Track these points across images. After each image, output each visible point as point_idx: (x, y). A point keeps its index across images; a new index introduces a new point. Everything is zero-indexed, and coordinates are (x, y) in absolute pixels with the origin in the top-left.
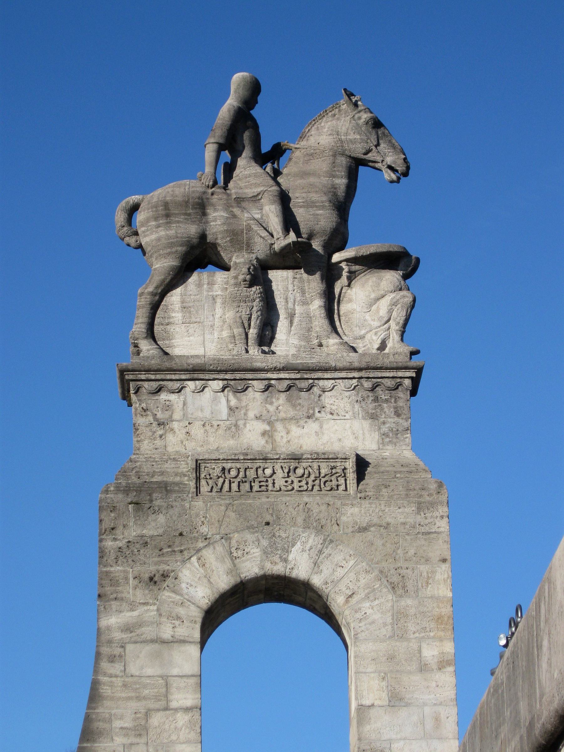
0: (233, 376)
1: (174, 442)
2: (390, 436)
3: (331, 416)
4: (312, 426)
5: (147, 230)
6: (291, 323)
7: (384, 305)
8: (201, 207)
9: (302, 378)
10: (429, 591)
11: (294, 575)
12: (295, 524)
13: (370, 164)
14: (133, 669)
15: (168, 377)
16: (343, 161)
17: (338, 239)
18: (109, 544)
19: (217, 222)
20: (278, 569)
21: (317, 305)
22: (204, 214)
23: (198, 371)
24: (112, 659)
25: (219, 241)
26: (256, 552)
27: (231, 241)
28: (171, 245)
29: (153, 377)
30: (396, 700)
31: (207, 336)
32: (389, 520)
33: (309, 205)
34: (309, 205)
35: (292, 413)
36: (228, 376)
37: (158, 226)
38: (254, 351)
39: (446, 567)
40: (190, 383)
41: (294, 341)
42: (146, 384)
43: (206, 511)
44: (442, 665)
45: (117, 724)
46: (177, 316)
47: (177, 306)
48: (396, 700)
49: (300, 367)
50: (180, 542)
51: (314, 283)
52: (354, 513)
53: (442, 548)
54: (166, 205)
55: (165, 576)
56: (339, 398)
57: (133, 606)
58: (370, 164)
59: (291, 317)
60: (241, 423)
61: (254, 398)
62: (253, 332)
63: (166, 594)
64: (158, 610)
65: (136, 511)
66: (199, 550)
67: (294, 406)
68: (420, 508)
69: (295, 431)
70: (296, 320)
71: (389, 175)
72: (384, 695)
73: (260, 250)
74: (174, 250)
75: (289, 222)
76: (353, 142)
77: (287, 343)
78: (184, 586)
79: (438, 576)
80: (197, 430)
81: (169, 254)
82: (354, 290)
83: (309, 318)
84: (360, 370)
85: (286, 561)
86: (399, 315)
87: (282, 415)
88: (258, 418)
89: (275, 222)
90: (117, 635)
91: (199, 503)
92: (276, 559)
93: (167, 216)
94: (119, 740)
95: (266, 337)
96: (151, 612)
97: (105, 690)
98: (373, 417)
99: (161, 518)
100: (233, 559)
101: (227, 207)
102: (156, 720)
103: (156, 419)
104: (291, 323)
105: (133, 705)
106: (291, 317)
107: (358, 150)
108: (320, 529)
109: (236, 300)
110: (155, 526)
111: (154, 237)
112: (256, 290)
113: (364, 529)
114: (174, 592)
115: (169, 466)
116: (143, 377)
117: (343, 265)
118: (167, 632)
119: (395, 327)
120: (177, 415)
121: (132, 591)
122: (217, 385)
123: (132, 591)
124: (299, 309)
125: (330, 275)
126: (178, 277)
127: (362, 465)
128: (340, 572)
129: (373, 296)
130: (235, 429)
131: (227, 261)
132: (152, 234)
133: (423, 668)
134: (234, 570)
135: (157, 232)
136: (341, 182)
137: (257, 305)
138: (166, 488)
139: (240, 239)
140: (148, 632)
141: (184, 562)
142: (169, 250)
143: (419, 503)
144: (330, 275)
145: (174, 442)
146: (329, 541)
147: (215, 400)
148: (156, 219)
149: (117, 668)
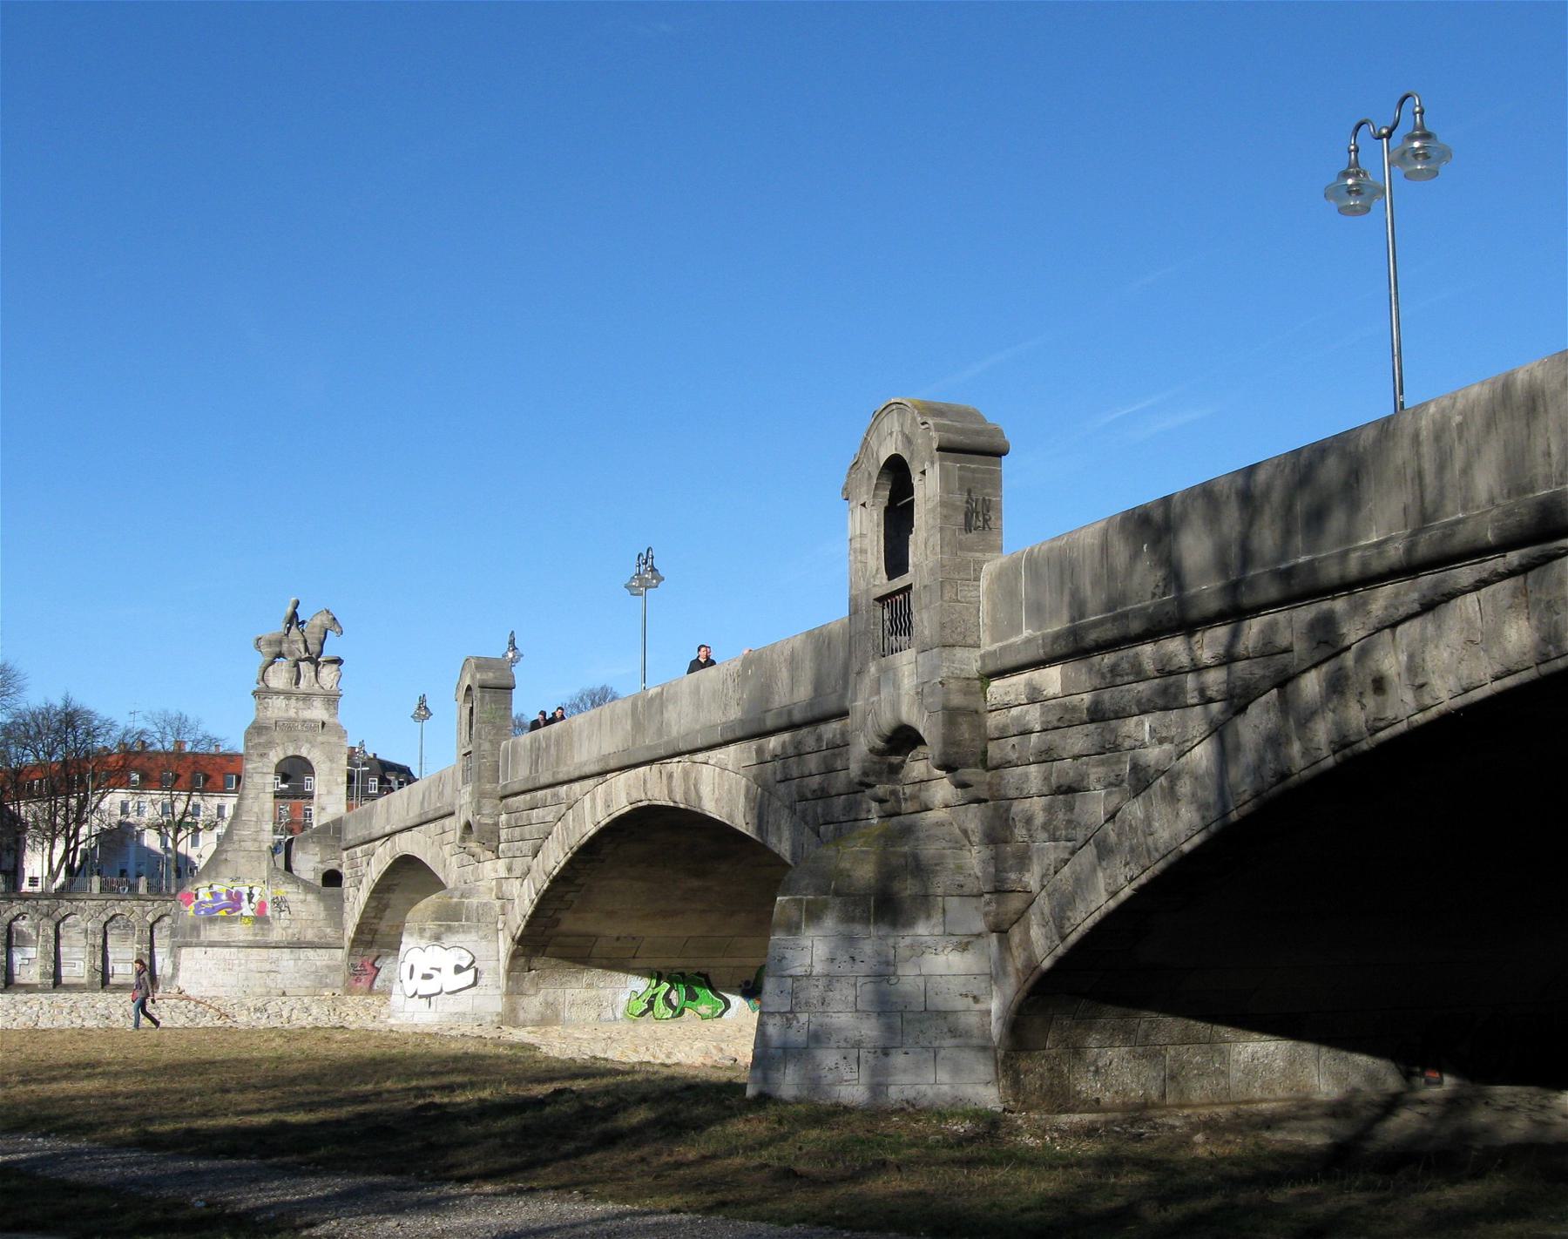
0: (287, 695)
8: (280, 642)
9: (307, 697)
19: (285, 647)
23: (278, 693)
30: (329, 793)
43: (277, 736)
48: (329, 793)
50: (270, 744)
51: (312, 667)
52: (320, 739)
56: (318, 703)
61: (293, 701)
73: (297, 655)
75: (307, 649)
77: (303, 684)
95: (297, 683)
121: (255, 758)
125: (317, 665)
126: (272, 663)
138: (267, 728)
139: (291, 653)
144: (317, 665)
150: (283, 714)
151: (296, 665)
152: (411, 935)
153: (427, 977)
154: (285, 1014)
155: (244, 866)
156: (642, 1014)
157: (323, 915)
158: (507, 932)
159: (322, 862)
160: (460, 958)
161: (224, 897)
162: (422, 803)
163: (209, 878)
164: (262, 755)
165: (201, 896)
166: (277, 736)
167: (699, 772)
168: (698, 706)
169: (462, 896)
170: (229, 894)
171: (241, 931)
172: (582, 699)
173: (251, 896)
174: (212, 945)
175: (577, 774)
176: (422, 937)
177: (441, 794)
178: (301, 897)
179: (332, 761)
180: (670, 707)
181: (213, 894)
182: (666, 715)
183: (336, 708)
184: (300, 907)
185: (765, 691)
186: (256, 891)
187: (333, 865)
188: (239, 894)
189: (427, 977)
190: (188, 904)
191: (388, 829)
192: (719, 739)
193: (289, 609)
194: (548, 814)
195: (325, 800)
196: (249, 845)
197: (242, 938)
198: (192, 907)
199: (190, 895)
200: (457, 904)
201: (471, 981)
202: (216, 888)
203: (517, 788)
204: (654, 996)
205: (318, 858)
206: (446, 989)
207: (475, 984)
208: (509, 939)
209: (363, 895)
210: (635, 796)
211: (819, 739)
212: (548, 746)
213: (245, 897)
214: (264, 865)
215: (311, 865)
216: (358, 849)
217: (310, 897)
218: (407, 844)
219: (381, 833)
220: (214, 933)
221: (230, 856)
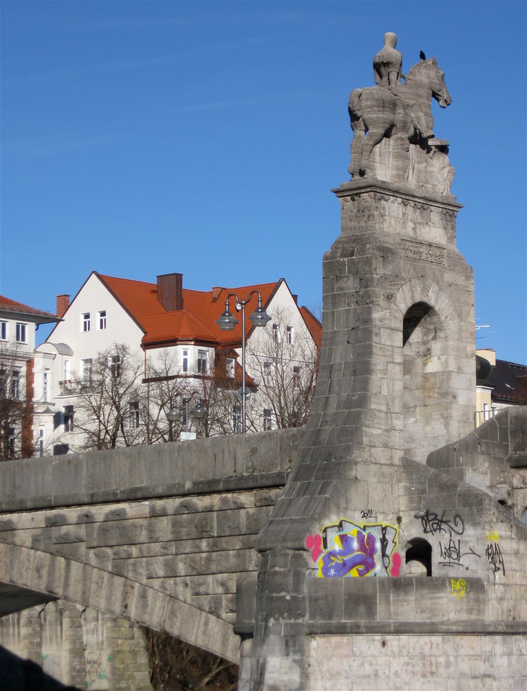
2: (451, 239)
3: (432, 225)
5: (372, 111)
6: (413, 172)
11: (429, 304)
12: (430, 279)
13: (437, 96)
15: (386, 193)
22: (395, 110)
25: (397, 125)
27: (402, 126)
28: (384, 123)
29: (381, 191)
31: (387, 172)
32: (457, 282)
35: (421, 221)
36: (404, 197)
37: (379, 111)
39: (473, 309)
40: (391, 197)
41: (414, 182)
42: (378, 194)
45: (379, 367)
46: (377, 158)
47: (378, 154)
49: (428, 198)
53: (472, 300)
58: (437, 96)
60: (406, 221)
64: (390, 312)
65: (384, 260)
66: (402, 285)
67: (422, 217)
70: (415, 171)
71: (442, 103)
72: (456, 367)
74: (385, 125)
76: (436, 84)
78: (398, 302)
79: (471, 313)
81: (383, 127)
82: (434, 161)
84: (444, 204)
85: (428, 296)
87: (419, 221)
88: (412, 220)
90: (378, 323)
92: (425, 294)
93: (383, 107)
94: (379, 375)
96: (387, 313)
98: (445, 228)
100: (413, 291)
103: (380, 214)
104: (413, 172)
105: (383, 358)
111: (375, 116)
113: (450, 285)
114: (395, 304)
116: (378, 191)
117: (433, 148)
122: (400, 200)
128: (444, 305)
129: (442, 166)
131: (392, 133)
132: (374, 114)
134: (413, 298)
135: (377, 114)
142: (383, 125)
143: (466, 276)
147: (398, 208)
148: (378, 107)
171: (450, 605)
174: (403, 629)
197: (453, 616)
198: (319, 563)
220: (408, 608)
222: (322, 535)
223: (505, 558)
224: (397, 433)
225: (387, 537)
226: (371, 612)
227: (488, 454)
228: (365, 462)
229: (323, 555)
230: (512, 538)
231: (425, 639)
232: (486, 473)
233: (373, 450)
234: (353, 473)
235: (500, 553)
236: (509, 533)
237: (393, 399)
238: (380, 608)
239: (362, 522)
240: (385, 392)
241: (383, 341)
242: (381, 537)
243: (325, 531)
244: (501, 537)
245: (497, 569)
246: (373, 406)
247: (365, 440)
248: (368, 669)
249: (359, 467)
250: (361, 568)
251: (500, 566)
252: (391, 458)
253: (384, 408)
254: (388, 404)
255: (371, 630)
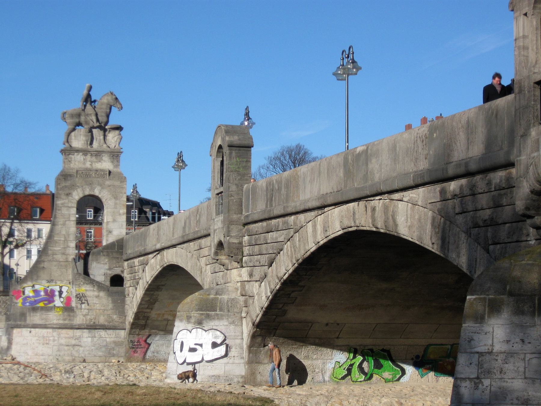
0: (85, 152)
1: (72, 165)
4: (100, 163)
7: (116, 138)
8: (79, 115)
9: (98, 154)
10: (122, 199)
14: (63, 212)
16: (109, 106)
17: (107, 123)
18: (59, 187)
19: (82, 119)
20: (92, 193)
21: (102, 137)
23: (78, 151)
24: (59, 210)
26: (88, 190)
30: (114, 221)
33: (102, 116)
34: (102, 116)
38: (89, 147)
44: (124, 214)
45: (60, 223)
46: (73, 138)
48: (114, 221)
50: (73, 187)
51: (102, 133)
52: (108, 183)
54: (72, 115)
55: (70, 194)
56: (106, 158)
57: (63, 199)
59: (97, 139)
62: (89, 143)
63: (70, 198)
68: (121, 182)
69: (97, 164)
73: (91, 124)
75: (98, 120)
77: (95, 144)
80: (77, 163)
83: (100, 140)
86: (118, 140)
89: (95, 120)
91: (77, 179)
94: (60, 226)
95: (91, 143)
96: (66, 201)
97: (57, 216)
98: (112, 162)
99: (69, 182)
101: (85, 116)
102: (67, 222)
106: (97, 139)
107: (112, 104)
108: (101, 185)
109: (85, 136)
110: (68, 183)
112: (90, 134)
113: (109, 186)
115: (71, 171)
118: (70, 205)
119: (118, 143)
120: (73, 160)
122: (81, 154)
123: (63, 197)
124: (98, 138)
125: (105, 130)
126: (74, 130)
127: (110, 172)
130: (84, 163)
133: (120, 214)
134: (84, 193)
136: (108, 111)
137: (90, 137)
138: (70, 176)
139: (87, 123)
140: (66, 205)
141: (74, 191)
145: (72, 165)
146: (102, 188)
149: (59, 212)
150: (81, 166)
151: (91, 131)
152: (181, 320)
153: (192, 350)
154: (86, 375)
155: (56, 272)
156: (343, 378)
157: (111, 306)
158: (249, 319)
159: (110, 269)
160: (216, 337)
161: (42, 293)
162: (184, 228)
163: (32, 280)
164: (68, 195)
165: (27, 293)
166: (78, 181)
167: (396, 206)
168: (395, 160)
169: (217, 294)
170: (46, 291)
171: (54, 317)
172: (282, 154)
173: (61, 292)
174: (35, 326)
175: (302, 208)
176: (189, 322)
177: (198, 221)
178: (96, 293)
179: (116, 198)
180: (374, 160)
181: (36, 291)
182: (370, 166)
183: (118, 161)
184: (96, 301)
185: (447, 149)
186: (64, 289)
187: (117, 271)
188: (53, 291)
189: (192, 350)
190: (17, 298)
191: (158, 246)
192: (411, 183)
193: (85, 92)
194: (280, 236)
195: (111, 226)
196: (59, 257)
197: (55, 322)
198: (20, 301)
199: (19, 292)
200: (213, 299)
201: (223, 353)
202: (37, 287)
203: (256, 217)
204: (352, 365)
205: (107, 267)
206: (206, 359)
207: (226, 355)
208: (251, 324)
209: (140, 293)
210: (347, 223)
211: (489, 183)
212: (279, 189)
213: (57, 293)
214: (70, 271)
215: (102, 271)
216: (136, 261)
217: (102, 294)
218: (172, 257)
219: (153, 249)
220: (36, 318)
221: (46, 265)
222: (22, 290)
223: (89, 299)
224: (71, 249)
225: (62, 290)
226: (25, 320)
227: (108, 255)
228: (49, 261)
229: (22, 298)
230: (94, 291)
231: (45, 331)
232: (106, 264)
233: (55, 256)
234: (42, 265)
235: (85, 296)
236: (92, 289)
237: (69, 235)
238: (28, 318)
239: (47, 285)
240: (64, 232)
241: (63, 212)
242: (59, 290)
243: (24, 288)
244: (86, 290)
245: (82, 303)
246: (55, 239)
247: (50, 252)
248: (25, 342)
249: (46, 263)
250: (46, 302)
251: (86, 302)
252: (67, 258)
253: (63, 239)
254: (65, 237)
255: (26, 326)
